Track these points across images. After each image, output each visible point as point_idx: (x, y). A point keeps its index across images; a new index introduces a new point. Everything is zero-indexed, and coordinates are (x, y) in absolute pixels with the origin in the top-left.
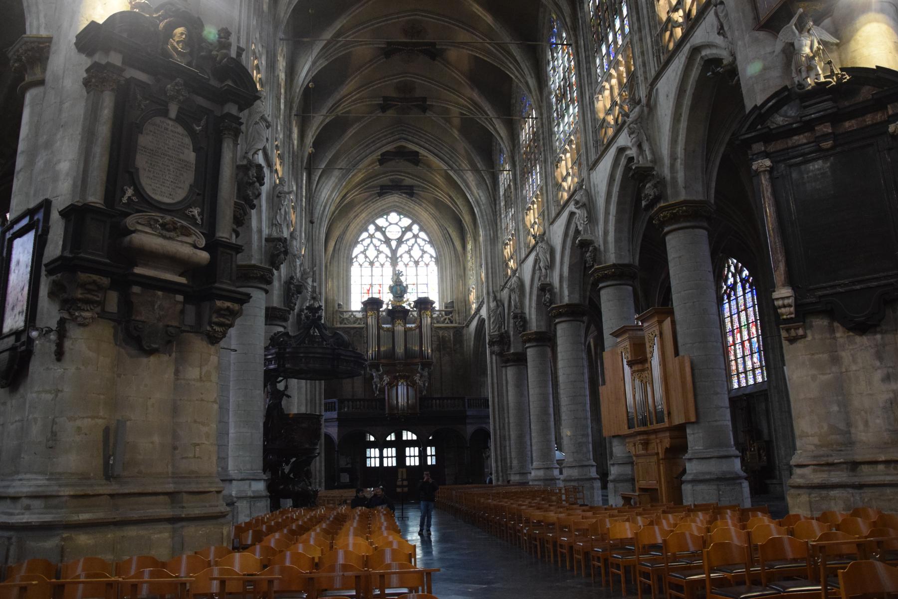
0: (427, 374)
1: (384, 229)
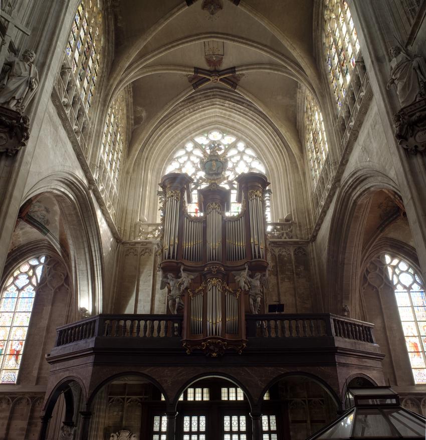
0: (258, 282)
1: (204, 147)
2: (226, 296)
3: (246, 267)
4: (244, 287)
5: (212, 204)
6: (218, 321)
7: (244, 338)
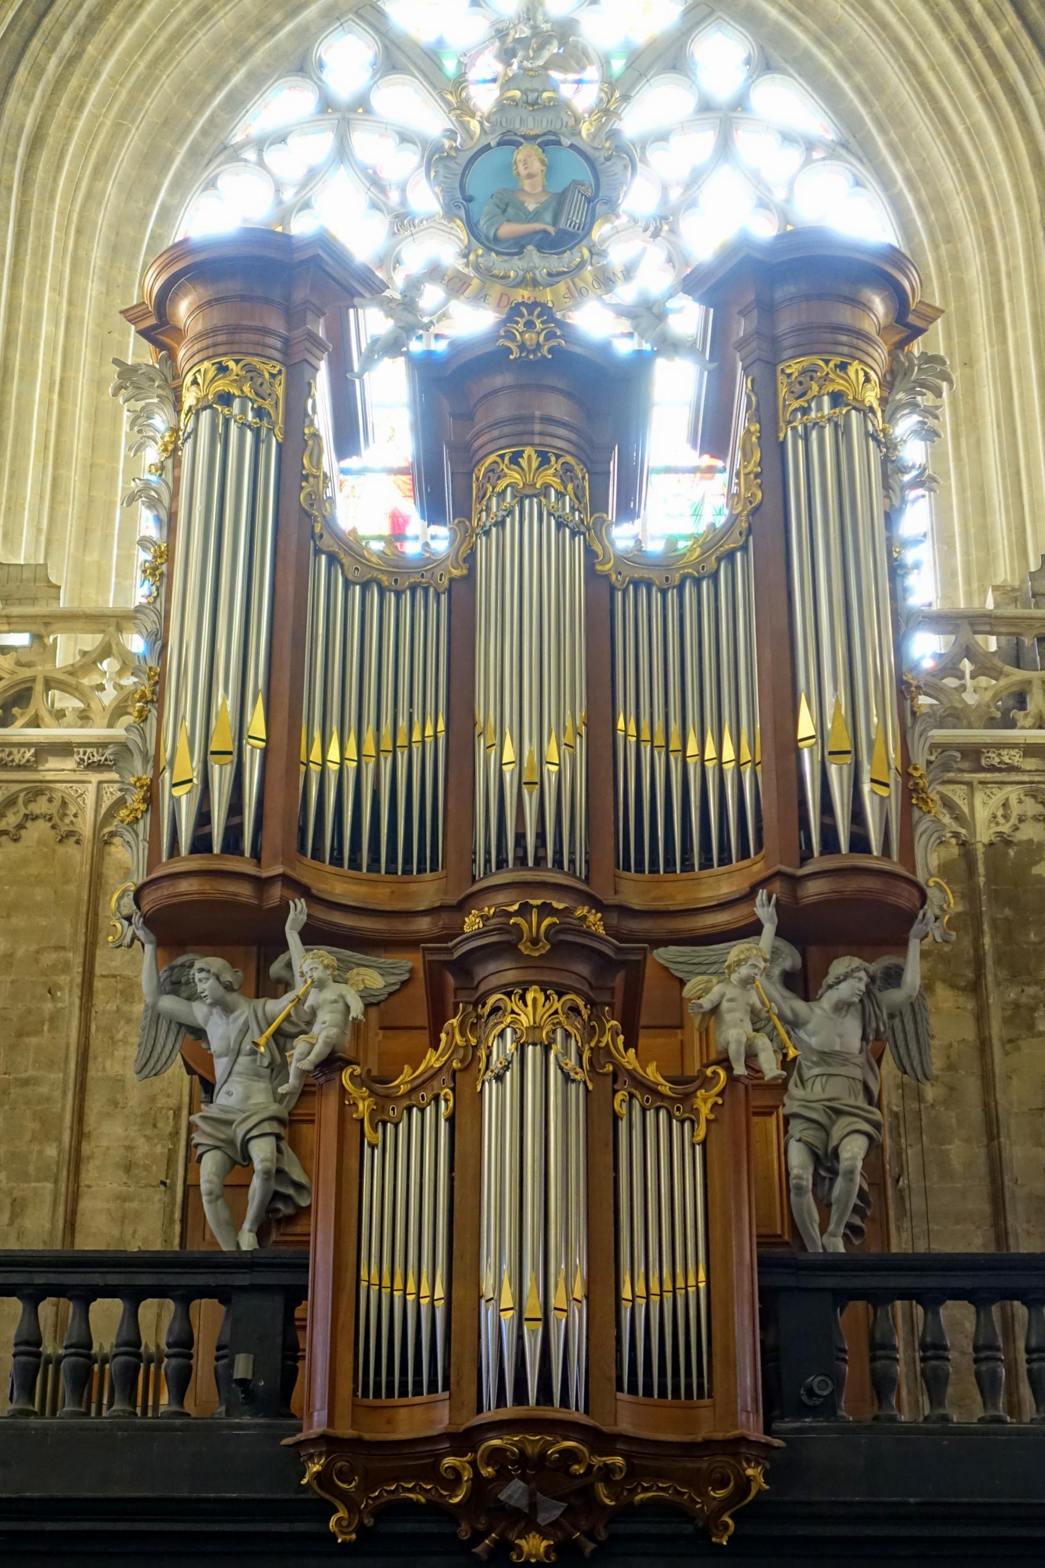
2: (616, 1118)
3: (764, 911)
4: (751, 1056)
5: (515, 459)
6: (557, 1299)
7: (752, 1428)
